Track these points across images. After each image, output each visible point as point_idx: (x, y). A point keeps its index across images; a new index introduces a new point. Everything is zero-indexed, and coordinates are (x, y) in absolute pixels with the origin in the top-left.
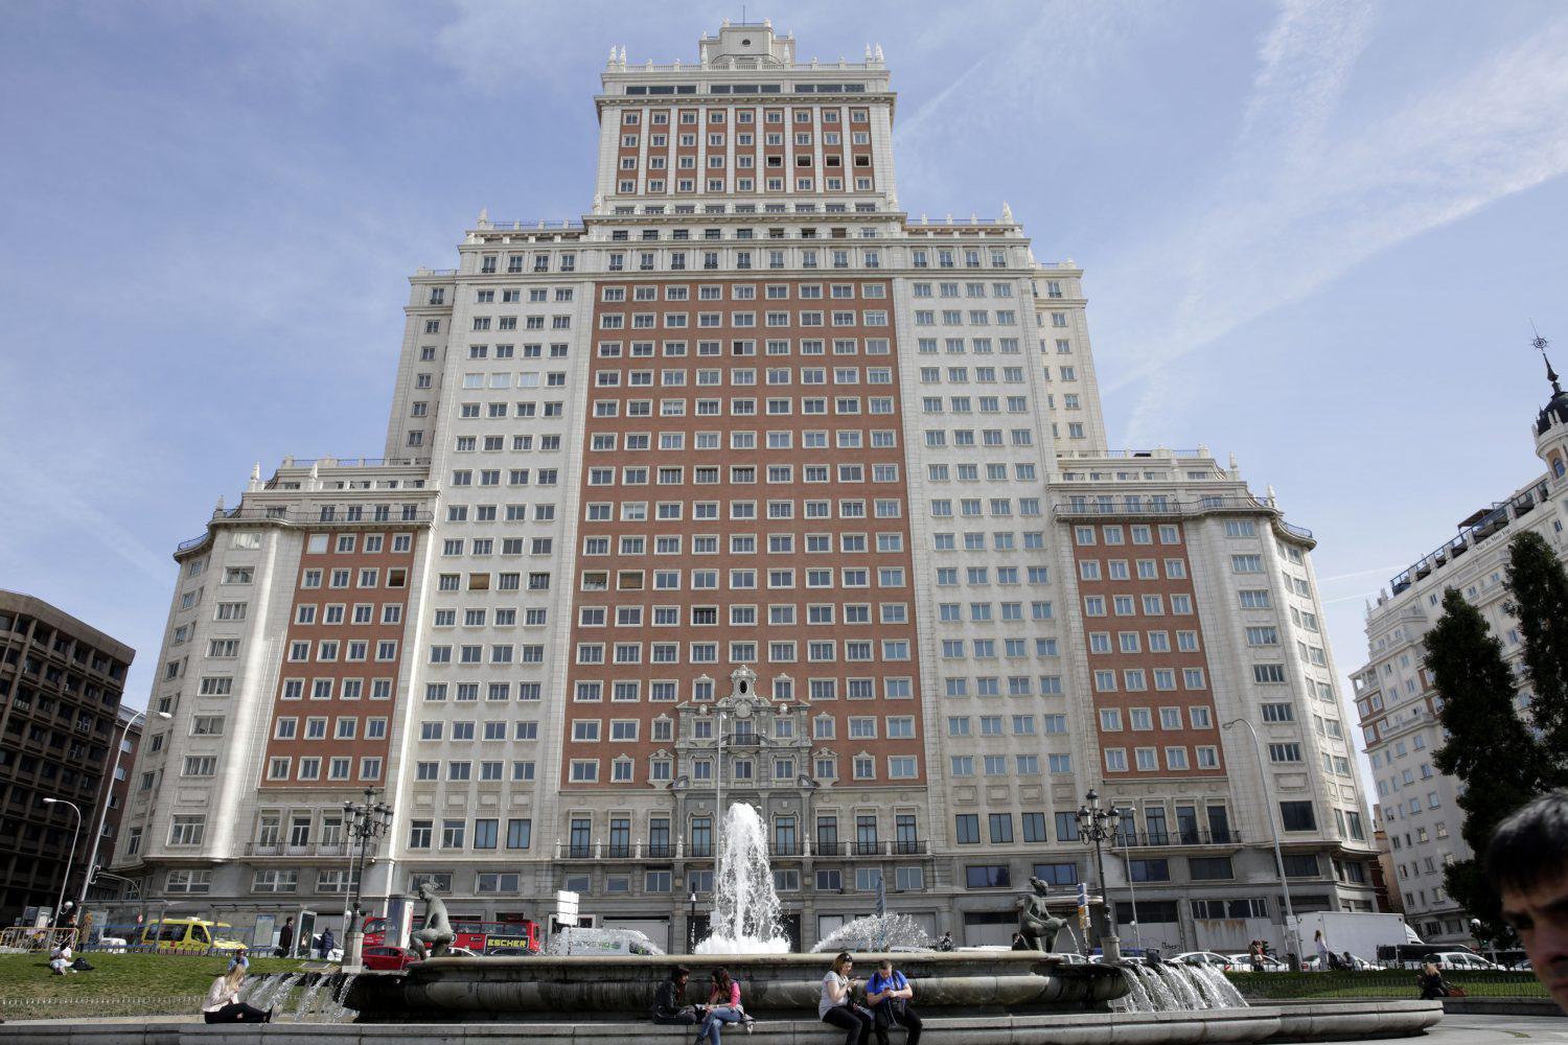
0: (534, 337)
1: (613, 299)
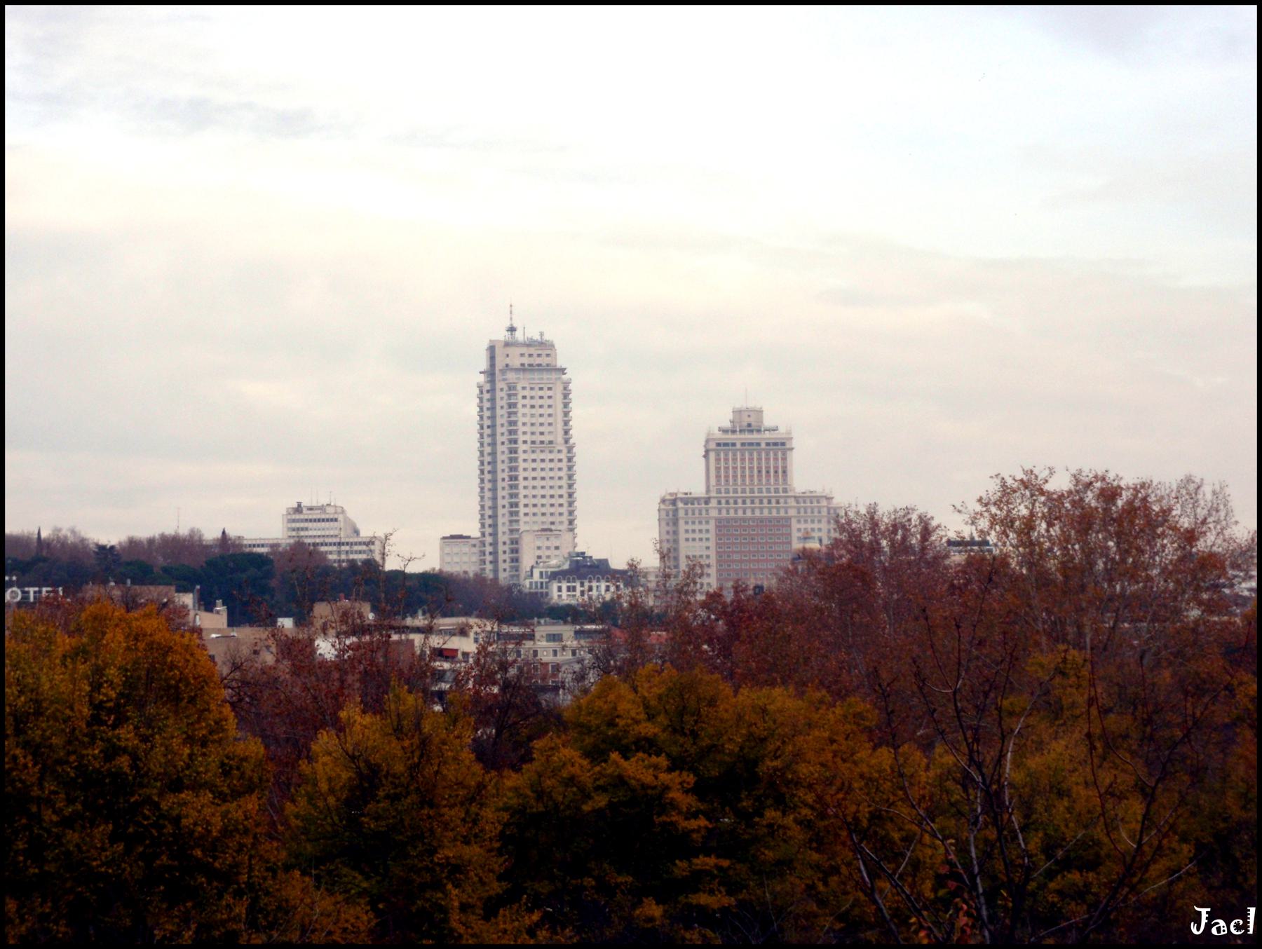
0: (701, 536)
1: (722, 525)
